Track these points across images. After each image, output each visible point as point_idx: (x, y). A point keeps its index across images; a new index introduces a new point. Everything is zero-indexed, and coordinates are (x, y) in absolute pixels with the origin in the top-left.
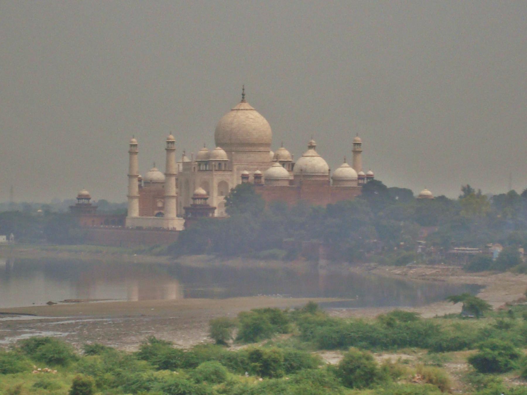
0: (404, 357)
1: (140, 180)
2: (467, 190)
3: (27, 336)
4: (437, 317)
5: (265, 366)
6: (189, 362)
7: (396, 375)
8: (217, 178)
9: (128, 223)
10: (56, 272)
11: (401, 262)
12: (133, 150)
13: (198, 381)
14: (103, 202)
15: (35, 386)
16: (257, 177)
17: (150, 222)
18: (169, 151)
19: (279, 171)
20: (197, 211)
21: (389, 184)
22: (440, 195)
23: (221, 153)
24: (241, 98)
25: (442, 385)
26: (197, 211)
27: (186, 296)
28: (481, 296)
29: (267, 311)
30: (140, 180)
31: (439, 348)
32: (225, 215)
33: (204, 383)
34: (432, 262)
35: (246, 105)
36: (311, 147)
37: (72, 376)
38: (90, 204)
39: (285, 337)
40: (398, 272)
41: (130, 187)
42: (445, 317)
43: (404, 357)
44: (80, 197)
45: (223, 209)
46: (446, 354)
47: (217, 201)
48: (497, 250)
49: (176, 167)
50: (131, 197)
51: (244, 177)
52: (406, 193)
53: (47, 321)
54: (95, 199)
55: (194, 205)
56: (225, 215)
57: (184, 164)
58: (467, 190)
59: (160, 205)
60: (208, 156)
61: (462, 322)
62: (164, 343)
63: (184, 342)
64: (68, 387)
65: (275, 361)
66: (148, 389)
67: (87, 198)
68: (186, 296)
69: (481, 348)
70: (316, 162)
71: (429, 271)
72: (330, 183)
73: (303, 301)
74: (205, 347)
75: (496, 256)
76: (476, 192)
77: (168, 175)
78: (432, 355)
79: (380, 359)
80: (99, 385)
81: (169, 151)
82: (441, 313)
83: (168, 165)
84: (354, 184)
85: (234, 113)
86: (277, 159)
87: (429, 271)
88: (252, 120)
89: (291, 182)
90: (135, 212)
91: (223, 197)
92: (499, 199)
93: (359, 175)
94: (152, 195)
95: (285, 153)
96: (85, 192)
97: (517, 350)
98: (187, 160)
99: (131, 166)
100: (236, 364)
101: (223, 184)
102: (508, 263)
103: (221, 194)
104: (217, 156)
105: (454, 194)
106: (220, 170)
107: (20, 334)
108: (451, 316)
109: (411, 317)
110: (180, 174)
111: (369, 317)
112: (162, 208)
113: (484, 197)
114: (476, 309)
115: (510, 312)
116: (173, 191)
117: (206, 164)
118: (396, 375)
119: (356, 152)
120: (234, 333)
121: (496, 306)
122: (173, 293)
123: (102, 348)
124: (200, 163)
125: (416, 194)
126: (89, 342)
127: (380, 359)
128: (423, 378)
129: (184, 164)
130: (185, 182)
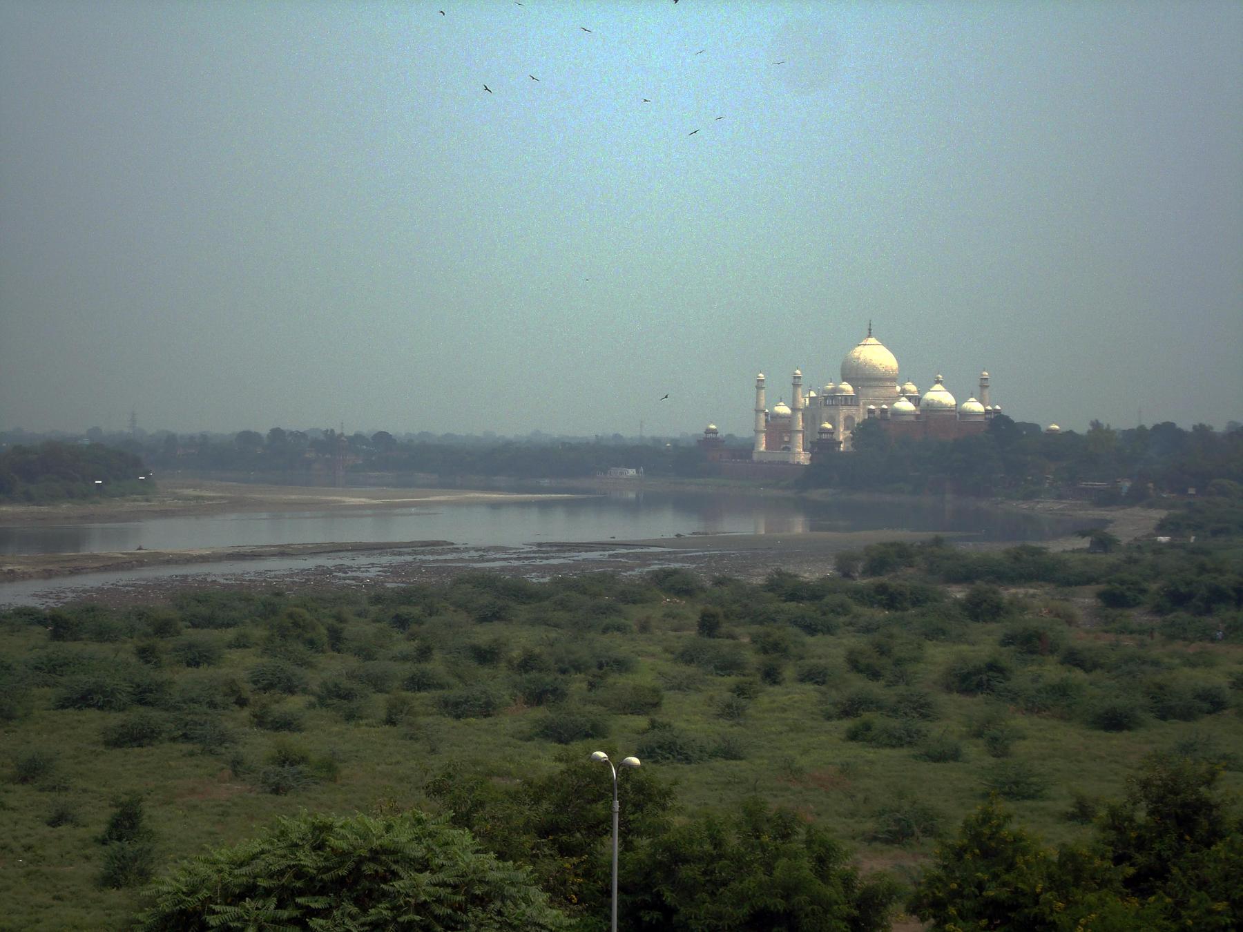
0: (1031, 591)
1: (766, 414)
2: (1096, 425)
3: (656, 567)
4: (1064, 551)
5: (890, 599)
6: (814, 594)
7: (1024, 609)
8: (844, 412)
9: (755, 457)
10: (683, 504)
11: (1028, 497)
12: (759, 385)
13: (824, 614)
14: (730, 436)
15: (665, 615)
16: (883, 411)
17: (778, 455)
18: (796, 385)
19: (905, 405)
20: (822, 446)
21: (1016, 418)
22: (1066, 429)
23: (847, 387)
24: (867, 332)
25: (1070, 620)
26: (822, 446)
27: (812, 529)
28: (1109, 530)
29: (892, 544)
30: (766, 414)
31: (1068, 583)
32: (851, 449)
33: (831, 615)
34: (1060, 497)
35: (872, 340)
36: (938, 382)
37: (700, 607)
38: (717, 439)
39: (910, 571)
40: (1025, 506)
41: (757, 421)
42: (1073, 551)
43: (1031, 591)
44: (708, 431)
45: (849, 444)
46: (1074, 588)
47: (842, 435)
48: (1126, 485)
49: (804, 401)
50: (757, 432)
51: (871, 411)
52: (1034, 428)
53: (674, 553)
54: (722, 433)
55: (820, 439)
56: (851, 449)
57: (811, 398)
58: (1096, 425)
59: (786, 439)
60: (835, 390)
61: (1090, 557)
62: (790, 576)
63: (811, 574)
64: (695, 618)
65: (901, 594)
66: (774, 620)
67: (714, 431)
68: (812, 529)
69: (1109, 582)
70: (941, 396)
71: (1057, 507)
72: (958, 417)
73: (929, 535)
74: (831, 579)
75: (1125, 490)
76: (1105, 426)
77: (794, 409)
78: (1060, 589)
79: (1007, 593)
80: (726, 616)
81: (796, 385)
82: (1069, 547)
83: (795, 400)
84: (981, 419)
85: (859, 349)
86: (903, 391)
87: (1057, 507)
88: (876, 355)
89: (917, 416)
90: (762, 448)
91: (848, 432)
92: (1129, 434)
93: (987, 411)
94: (778, 429)
95: (911, 387)
96: (713, 427)
97: (1145, 585)
98: (813, 394)
99: (758, 402)
100: (861, 596)
101: (849, 419)
102: (1137, 497)
103: (846, 428)
104: (843, 390)
105: (1082, 428)
106: (846, 404)
107: (650, 565)
108: (1080, 551)
109: (1038, 552)
110: (806, 408)
111: (995, 549)
112: (789, 442)
113: (1114, 432)
114: (1104, 543)
115: (1139, 547)
116: (800, 425)
117: (833, 399)
118: (1024, 609)
119: (983, 387)
120: (860, 566)
121: (1124, 541)
122: (798, 526)
123: (730, 580)
124: (826, 398)
125: (1043, 429)
126: (717, 574)
127: (1007, 593)
128: (1051, 612)
129: (811, 398)
130: (812, 414)
